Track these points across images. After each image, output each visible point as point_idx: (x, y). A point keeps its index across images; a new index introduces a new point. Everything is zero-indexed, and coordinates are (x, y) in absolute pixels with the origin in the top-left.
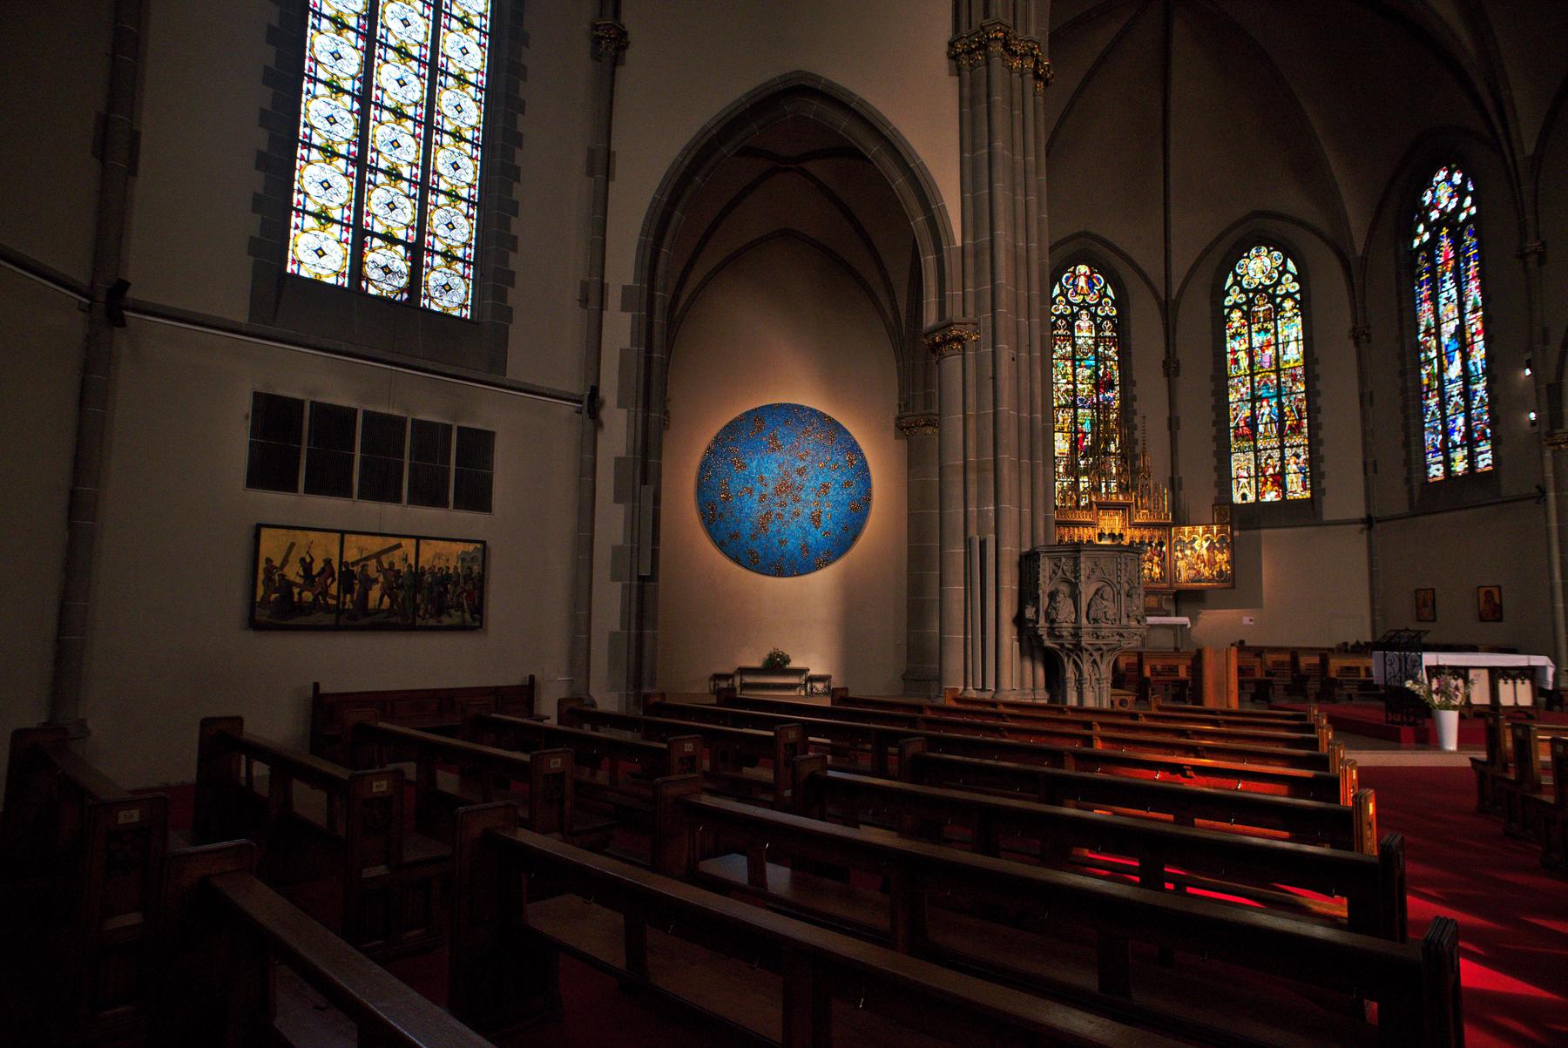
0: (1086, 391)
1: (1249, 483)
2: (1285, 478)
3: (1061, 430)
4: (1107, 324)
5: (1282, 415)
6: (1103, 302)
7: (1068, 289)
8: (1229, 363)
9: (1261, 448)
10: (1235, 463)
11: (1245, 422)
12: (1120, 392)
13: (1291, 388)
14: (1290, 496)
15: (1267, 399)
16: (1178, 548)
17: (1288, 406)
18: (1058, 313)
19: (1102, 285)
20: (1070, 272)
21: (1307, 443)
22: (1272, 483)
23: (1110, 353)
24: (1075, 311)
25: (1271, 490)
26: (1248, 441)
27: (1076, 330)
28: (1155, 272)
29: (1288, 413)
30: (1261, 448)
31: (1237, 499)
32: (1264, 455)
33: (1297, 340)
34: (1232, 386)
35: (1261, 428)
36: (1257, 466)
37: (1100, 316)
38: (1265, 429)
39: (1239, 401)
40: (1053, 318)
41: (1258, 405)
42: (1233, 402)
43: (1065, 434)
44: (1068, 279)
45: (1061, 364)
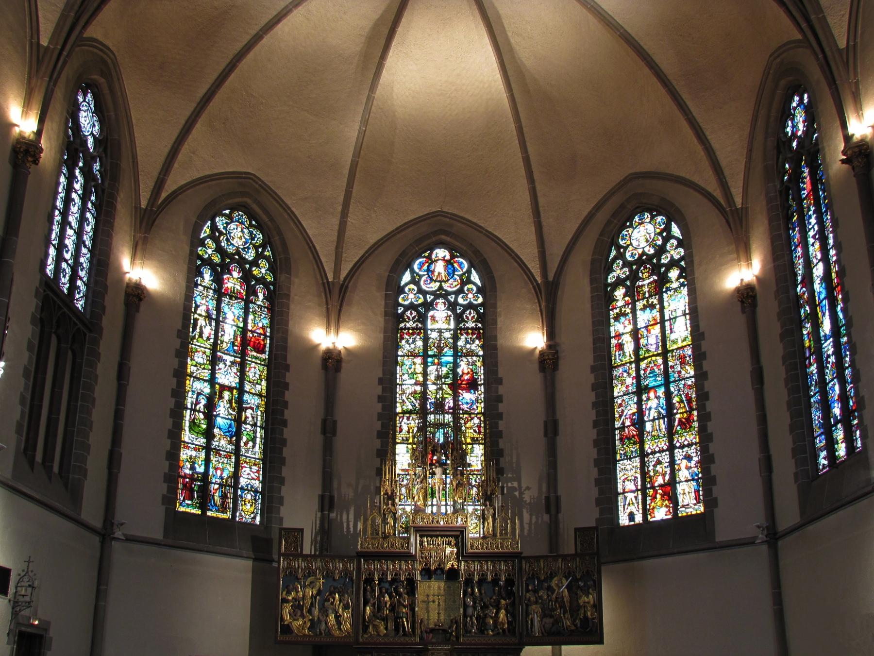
1: (636, 498)
2: (676, 489)
3: (405, 441)
4: (471, 314)
5: (670, 406)
6: (466, 289)
8: (613, 349)
9: (649, 451)
10: (622, 474)
11: (632, 419)
13: (679, 372)
15: (653, 388)
17: (677, 395)
18: (406, 303)
19: (465, 270)
21: (697, 440)
22: (662, 496)
23: (473, 347)
24: (429, 300)
25: (661, 506)
26: (634, 444)
27: (429, 321)
28: (530, 256)
29: (677, 404)
30: (649, 451)
31: (624, 520)
32: (652, 460)
33: (685, 314)
34: (617, 378)
35: (648, 427)
36: (644, 474)
37: (461, 305)
38: (653, 427)
39: (624, 395)
40: (400, 310)
41: (644, 397)
42: (618, 397)
43: (410, 446)
44: (421, 265)
45: (408, 361)
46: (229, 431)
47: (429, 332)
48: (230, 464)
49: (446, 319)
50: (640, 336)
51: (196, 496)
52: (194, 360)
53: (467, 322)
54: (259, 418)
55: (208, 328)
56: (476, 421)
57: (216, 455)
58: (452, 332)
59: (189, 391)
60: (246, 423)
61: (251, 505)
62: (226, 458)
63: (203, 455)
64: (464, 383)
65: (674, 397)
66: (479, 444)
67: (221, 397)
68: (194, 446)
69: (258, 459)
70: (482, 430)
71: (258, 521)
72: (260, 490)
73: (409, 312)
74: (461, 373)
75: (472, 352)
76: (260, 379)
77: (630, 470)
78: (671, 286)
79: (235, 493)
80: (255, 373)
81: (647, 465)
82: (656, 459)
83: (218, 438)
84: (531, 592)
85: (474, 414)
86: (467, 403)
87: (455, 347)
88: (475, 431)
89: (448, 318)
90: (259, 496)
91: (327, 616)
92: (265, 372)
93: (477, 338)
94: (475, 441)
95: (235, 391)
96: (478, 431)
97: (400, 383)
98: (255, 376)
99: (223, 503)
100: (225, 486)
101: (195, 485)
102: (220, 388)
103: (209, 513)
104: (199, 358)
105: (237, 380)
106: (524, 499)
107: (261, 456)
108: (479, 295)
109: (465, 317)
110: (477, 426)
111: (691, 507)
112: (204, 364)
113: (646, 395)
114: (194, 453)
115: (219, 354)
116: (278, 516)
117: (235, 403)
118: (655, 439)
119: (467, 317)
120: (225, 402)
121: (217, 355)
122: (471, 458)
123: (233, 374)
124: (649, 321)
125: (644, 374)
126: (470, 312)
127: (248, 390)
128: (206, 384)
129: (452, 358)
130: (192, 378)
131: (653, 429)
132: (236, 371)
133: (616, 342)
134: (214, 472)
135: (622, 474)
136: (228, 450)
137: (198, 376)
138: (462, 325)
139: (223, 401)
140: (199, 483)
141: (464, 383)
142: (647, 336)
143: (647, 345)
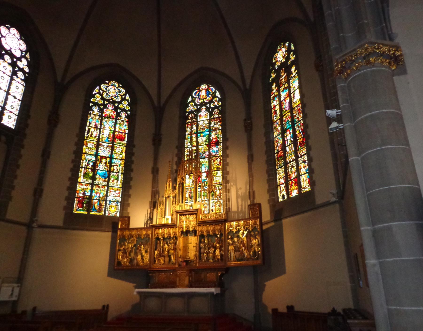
0: (203, 149)
6: (214, 100)
7: (195, 98)
12: (222, 146)
13: (298, 118)
14: (304, 191)
16: (230, 237)
19: (213, 92)
20: (197, 89)
22: (295, 184)
23: (217, 126)
27: (199, 118)
29: (298, 135)
30: (288, 162)
38: (289, 149)
41: (285, 135)
44: (196, 93)
46: (104, 176)
47: (199, 122)
48: (104, 191)
49: (206, 116)
50: (282, 105)
51: (85, 206)
52: (88, 147)
53: (214, 115)
54: (121, 169)
55: (96, 132)
56: (219, 160)
57: (97, 187)
58: (208, 121)
59: (84, 160)
60: (113, 172)
61: (115, 208)
62: (102, 188)
63: (90, 187)
64: (213, 143)
65: (297, 131)
66: (220, 170)
67: (101, 162)
68: (85, 184)
69: (119, 187)
70: (221, 164)
71: (118, 215)
72: (120, 201)
73: (191, 115)
74: (212, 139)
75: (217, 128)
76: (122, 152)
77: (282, 173)
78: (293, 75)
79: (106, 203)
80: (119, 150)
81: (288, 169)
82: (291, 165)
83: (98, 180)
84: (230, 239)
85: (218, 156)
86: (215, 152)
87: (209, 127)
88: (218, 165)
89: (207, 115)
90: (119, 204)
91: (137, 256)
92: (125, 149)
93: (219, 122)
94: (218, 169)
95: (108, 159)
96: (219, 164)
97: (187, 147)
98: (119, 151)
99: (100, 208)
100: (101, 200)
101: (85, 201)
102: (100, 158)
103: (91, 213)
104: (90, 145)
105: (110, 154)
106: (239, 194)
107: (121, 186)
108: (220, 102)
109: (214, 113)
110: (219, 162)
111: (307, 188)
112: (93, 148)
113: (286, 133)
114: (85, 187)
115: (100, 143)
116: (127, 212)
117: (108, 164)
118: (290, 155)
119: (214, 113)
120: (103, 163)
121: (99, 143)
122: (216, 177)
123: (107, 151)
124: (285, 96)
125: (285, 123)
126: (216, 110)
127: (115, 158)
128: (93, 156)
129: (208, 132)
130: (86, 154)
131: (289, 150)
132: (109, 150)
133: (274, 110)
134: (96, 195)
135: (279, 175)
136: (103, 184)
137: (89, 153)
138: (212, 117)
139: (102, 163)
140: (87, 200)
141: (213, 143)
142: (285, 104)
143: (285, 108)
